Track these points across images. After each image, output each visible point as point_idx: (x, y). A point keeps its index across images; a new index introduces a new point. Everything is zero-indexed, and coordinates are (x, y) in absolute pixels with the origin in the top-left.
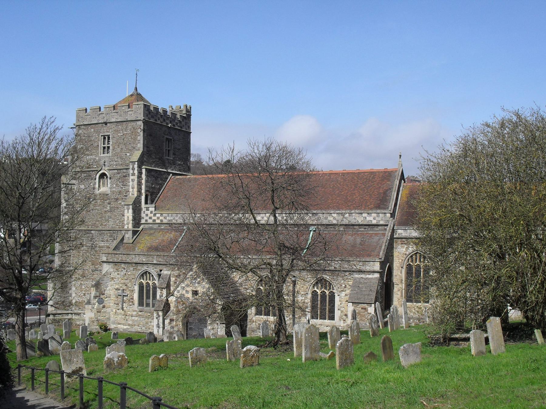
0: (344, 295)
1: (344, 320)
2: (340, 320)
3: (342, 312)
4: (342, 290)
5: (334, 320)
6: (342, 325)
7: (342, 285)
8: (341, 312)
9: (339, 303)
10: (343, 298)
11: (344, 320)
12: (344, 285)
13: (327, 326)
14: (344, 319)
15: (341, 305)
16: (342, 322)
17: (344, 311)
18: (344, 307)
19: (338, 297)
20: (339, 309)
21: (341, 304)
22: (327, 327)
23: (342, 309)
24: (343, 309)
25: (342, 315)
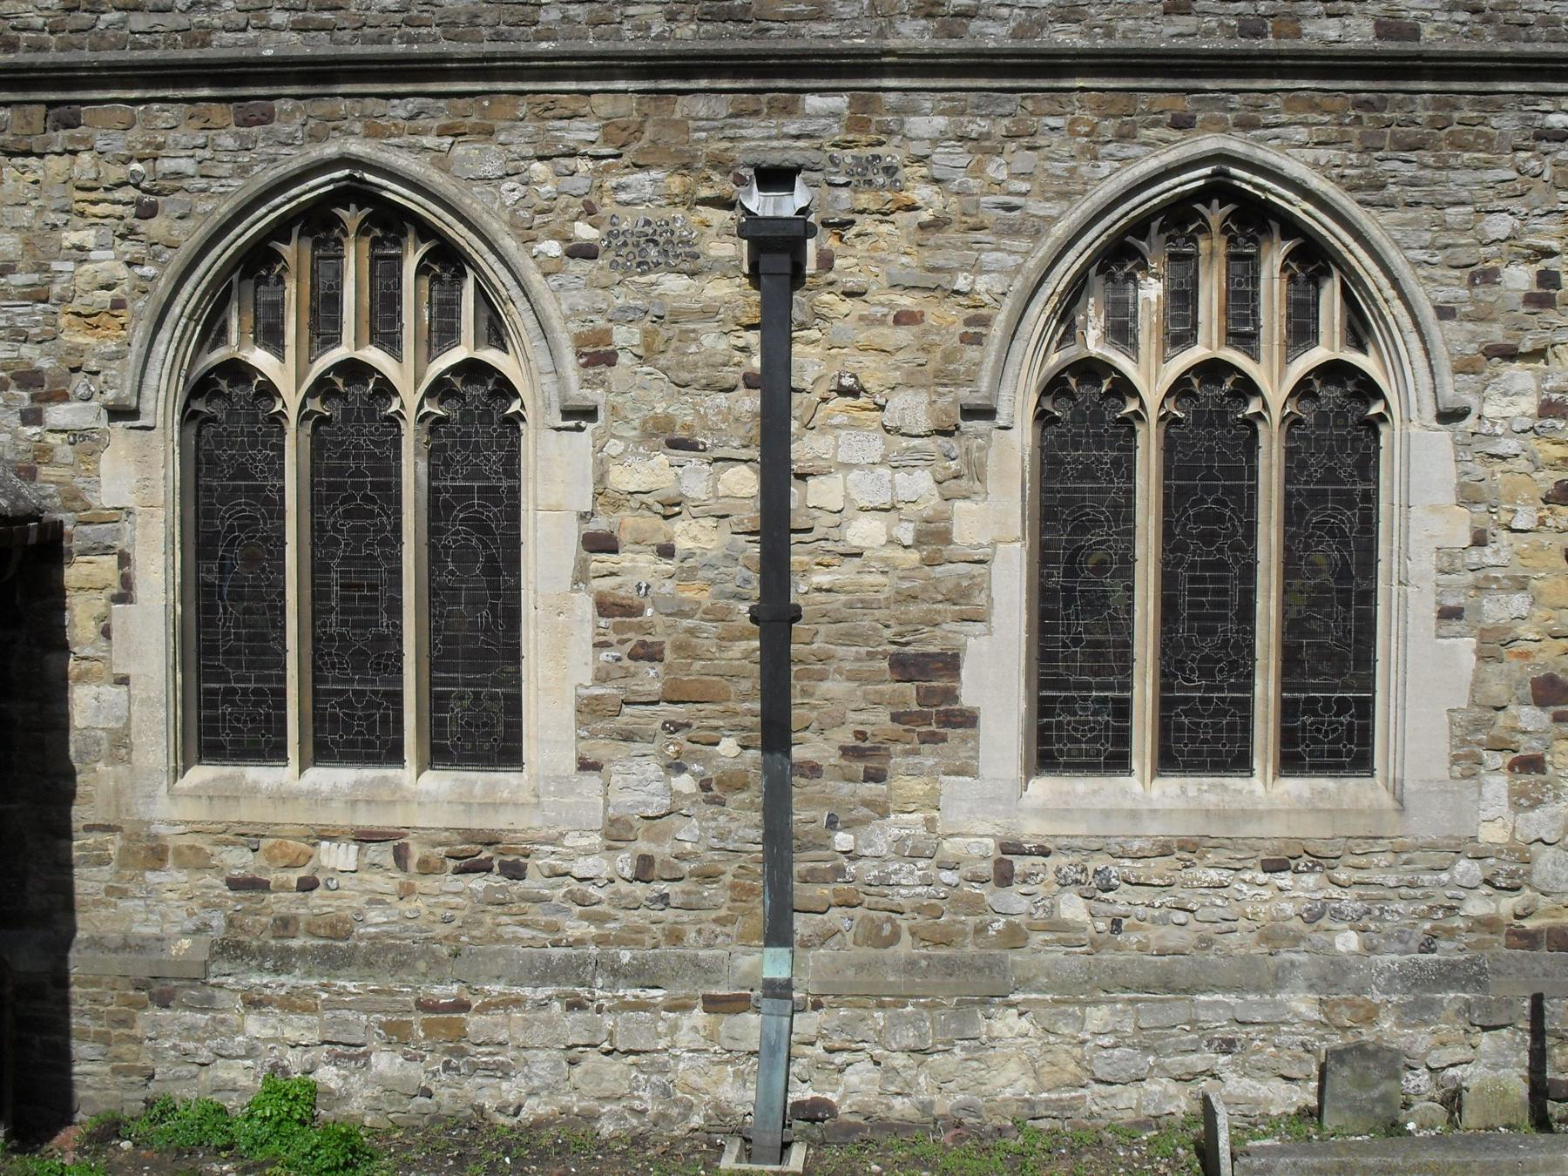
0: (1529, 405)
1: (1532, 764)
2: (1467, 763)
3: (1494, 645)
4: (1497, 333)
5: (1362, 763)
6: (1492, 834)
7: (1490, 277)
8: (1483, 657)
9: (1457, 528)
10: (1508, 446)
11: (1532, 764)
12: (1520, 278)
13: (1274, 866)
14: (1528, 747)
15: (1487, 555)
16: (1497, 785)
17: (1526, 631)
18: (1521, 585)
19: (1444, 437)
20: (1448, 614)
21: (1480, 540)
22: (1285, 879)
23: (1499, 609)
24: (1518, 603)
25: (1497, 689)
